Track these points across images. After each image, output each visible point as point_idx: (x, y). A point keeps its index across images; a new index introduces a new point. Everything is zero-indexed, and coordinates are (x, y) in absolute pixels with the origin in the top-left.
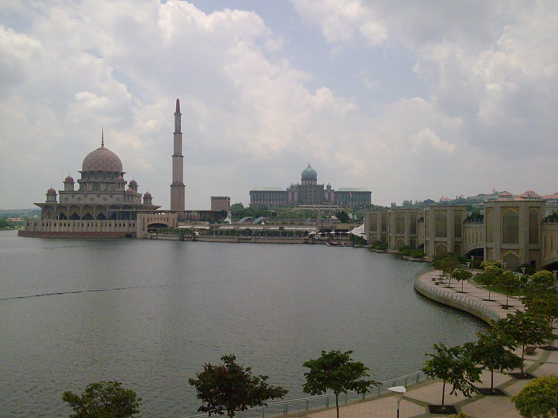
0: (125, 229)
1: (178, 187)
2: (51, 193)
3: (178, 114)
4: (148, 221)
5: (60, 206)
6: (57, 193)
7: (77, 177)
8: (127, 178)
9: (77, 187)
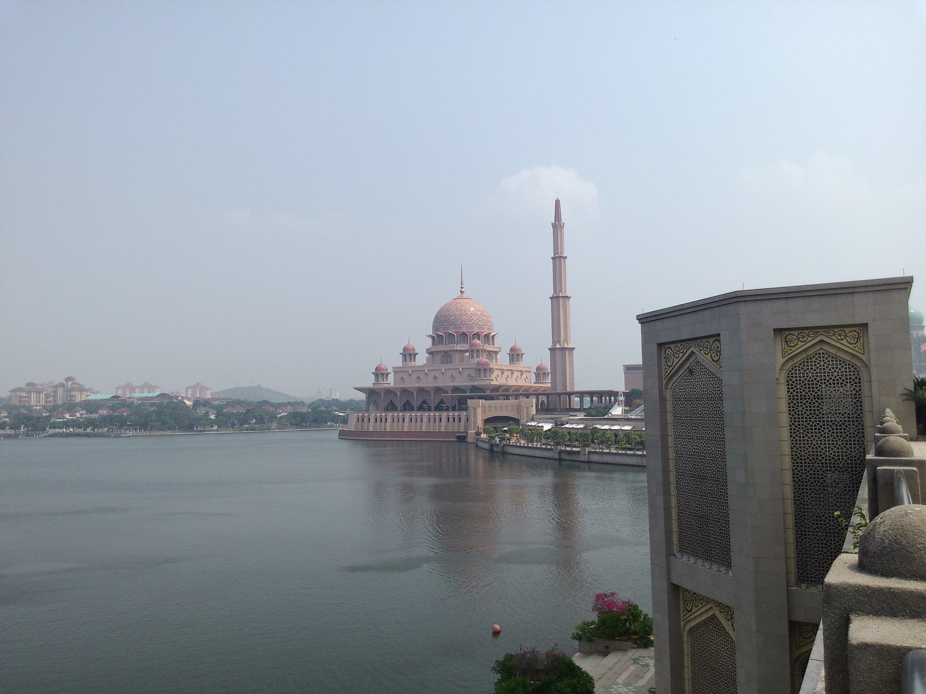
0: (454, 427)
1: (560, 352)
2: (380, 373)
3: (557, 225)
4: (484, 412)
5: (389, 391)
6: (390, 370)
7: (423, 345)
8: (503, 344)
9: (422, 359)
